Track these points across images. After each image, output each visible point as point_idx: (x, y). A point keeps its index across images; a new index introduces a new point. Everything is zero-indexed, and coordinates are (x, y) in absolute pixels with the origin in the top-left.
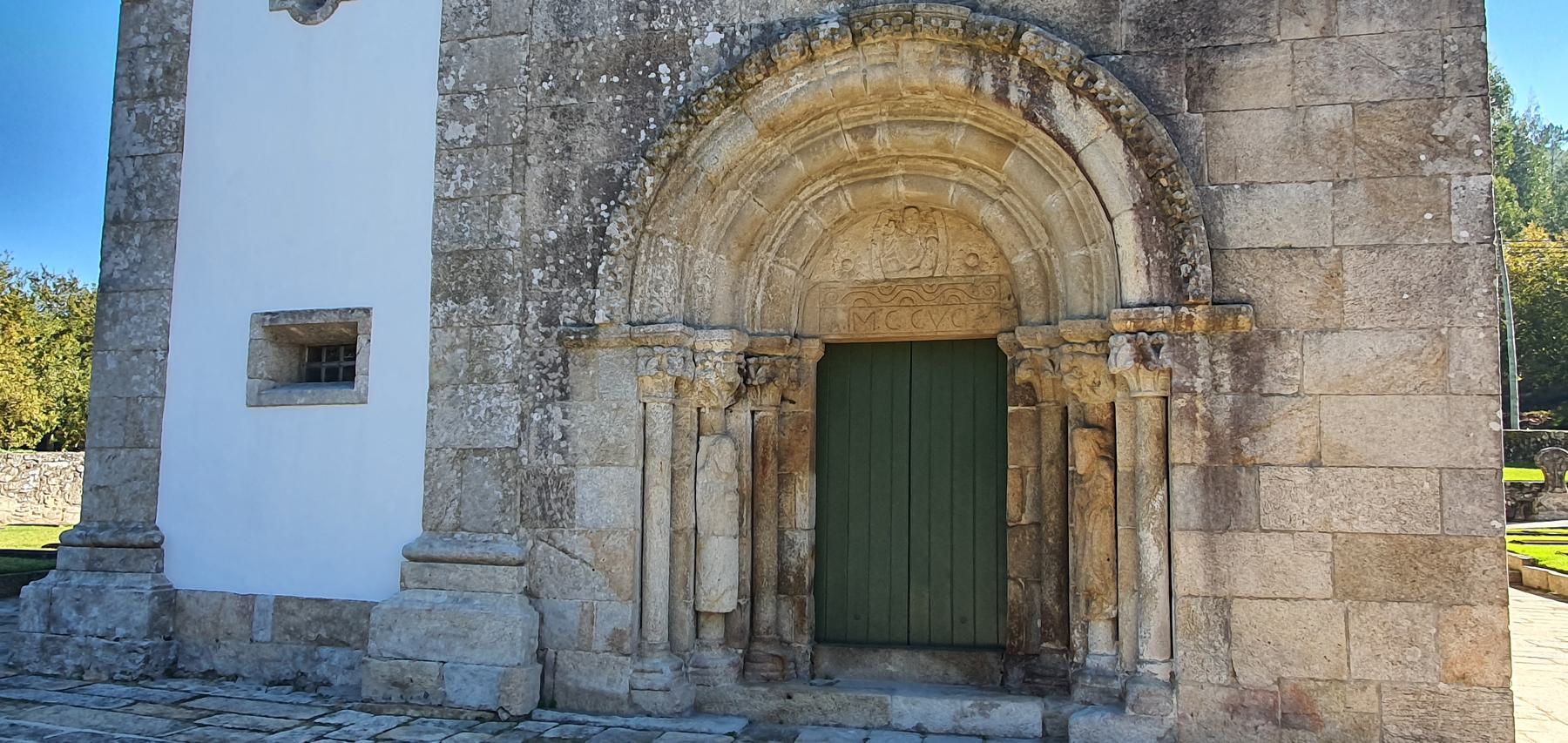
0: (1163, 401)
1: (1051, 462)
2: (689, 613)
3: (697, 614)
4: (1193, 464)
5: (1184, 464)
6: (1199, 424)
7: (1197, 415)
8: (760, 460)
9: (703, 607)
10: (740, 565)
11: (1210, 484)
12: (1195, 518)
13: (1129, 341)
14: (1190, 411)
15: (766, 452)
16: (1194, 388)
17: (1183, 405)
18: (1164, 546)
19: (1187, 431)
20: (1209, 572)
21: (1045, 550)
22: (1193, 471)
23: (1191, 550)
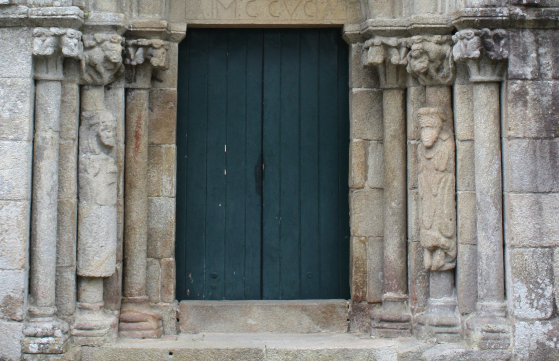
0: (497, 86)
1: (394, 137)
2: (71, 277)
3: (79, 279)
4: (525, 138)
5: (518, 138)
6: (529, 105)
7: (528, 97)
8: (133, 134)
9: (85, 272)
10: (118, 232)
11: (538, 153)
12: (527, 182)
13: (476, 35)
14: (521, 95)
15: (139, 126)
16: (525, 75)
17: (517, 89)
18: (499, 207)
19: (521, 111)
20: (538, 226)
21: (390, 212)
22: (525, 143)
23: (524, 209)
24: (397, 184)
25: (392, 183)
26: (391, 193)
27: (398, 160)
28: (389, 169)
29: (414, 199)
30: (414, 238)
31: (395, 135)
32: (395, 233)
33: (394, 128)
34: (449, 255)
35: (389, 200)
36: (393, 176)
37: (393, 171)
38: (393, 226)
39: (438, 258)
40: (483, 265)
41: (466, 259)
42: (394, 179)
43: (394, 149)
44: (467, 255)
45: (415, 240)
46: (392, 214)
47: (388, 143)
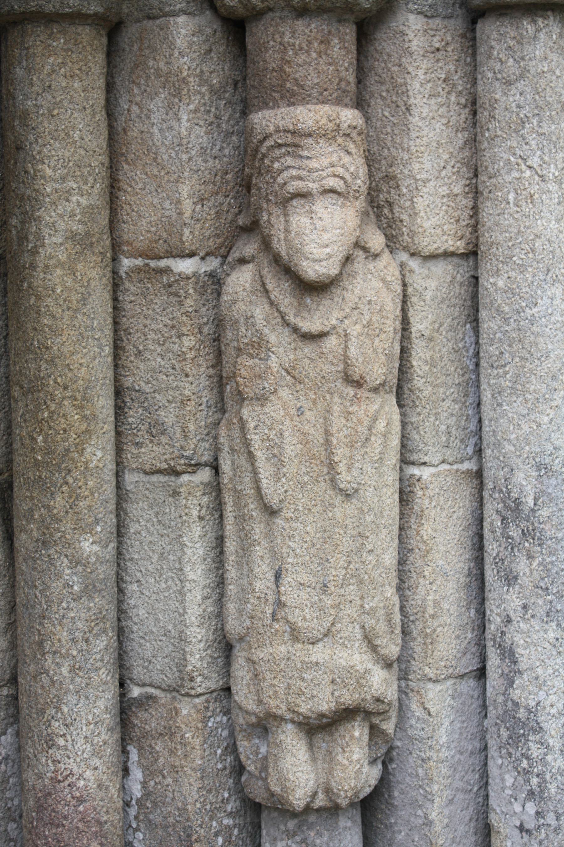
24: (99, 454)
25: (82, 452)
26: (78, 497)
27: (100, 347)
28: (65, 388)
29: (195, 513)
30: (199, 679)
31: (88, 234)
32: (97, 669)
33: (84, 201)
34: (383, 733)
35: (67, 526)
36: (84, 418)
37: (84, 398)
38: (87, 641)
39: (355, 757)
40: (549, 758)
41: (444, 739)
42: (87, 431)
43: (84, 300)
44: (447, 723)
45: (200, 690)
46: (85, 590)
47: (59, 272)
